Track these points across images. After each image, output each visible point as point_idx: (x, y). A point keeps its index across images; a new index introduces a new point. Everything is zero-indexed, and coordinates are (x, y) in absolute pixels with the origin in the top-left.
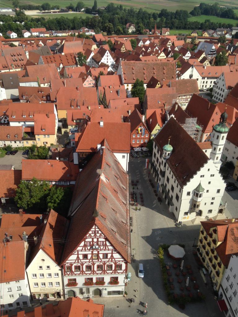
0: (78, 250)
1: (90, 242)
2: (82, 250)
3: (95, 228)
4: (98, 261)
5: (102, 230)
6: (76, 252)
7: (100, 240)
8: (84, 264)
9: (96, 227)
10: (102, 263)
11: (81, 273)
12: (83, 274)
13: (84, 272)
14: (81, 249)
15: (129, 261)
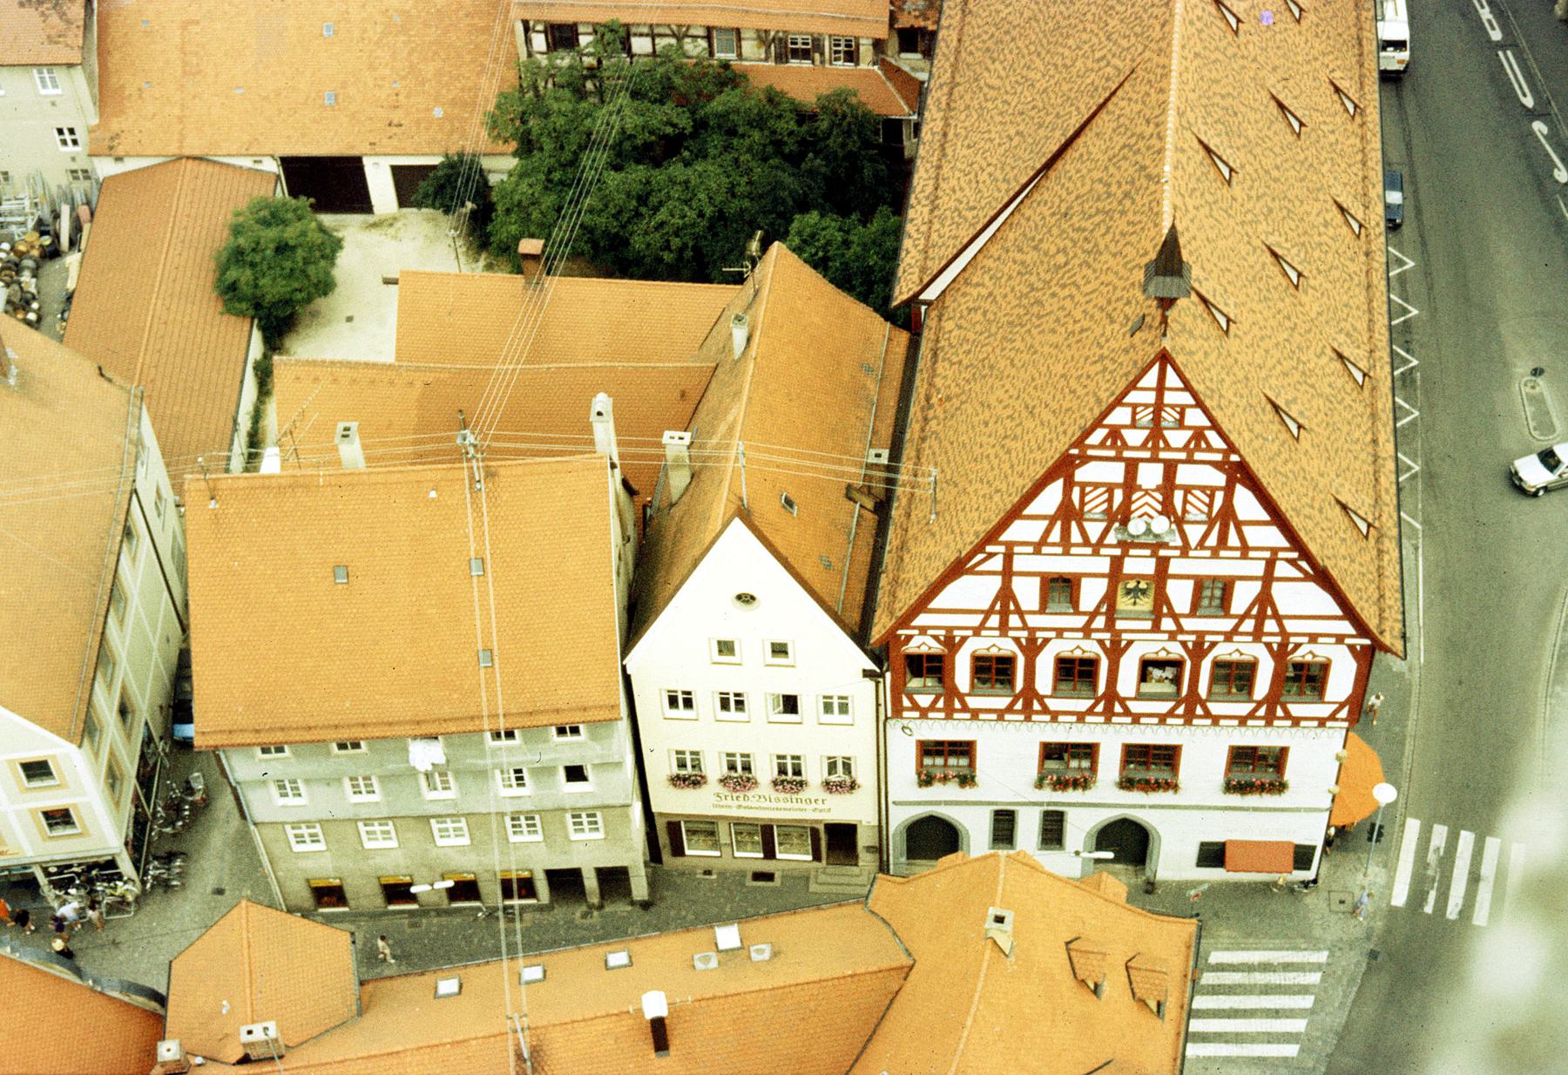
0: (1010, 546)
1: (1110, 488)
2: (1038, 548)
3: (1160, 389)
4: (1156, 628)
5: (1208, 403)
6: (991, 555)
7: (1184, 475)
8: (1046, 641)
9: (1172, 379)
10: (1184, 644)
11: (1019, 706)
12: (1028, 712)
13: (1041, 699)
14: (1036, 539)
15: (1387, 639)
